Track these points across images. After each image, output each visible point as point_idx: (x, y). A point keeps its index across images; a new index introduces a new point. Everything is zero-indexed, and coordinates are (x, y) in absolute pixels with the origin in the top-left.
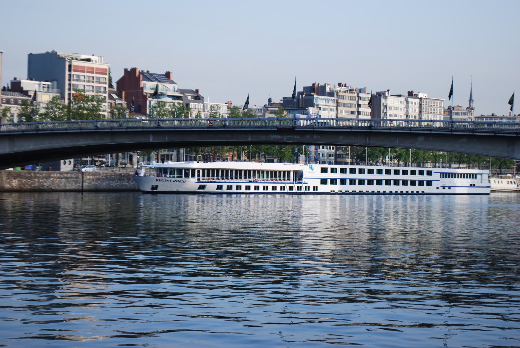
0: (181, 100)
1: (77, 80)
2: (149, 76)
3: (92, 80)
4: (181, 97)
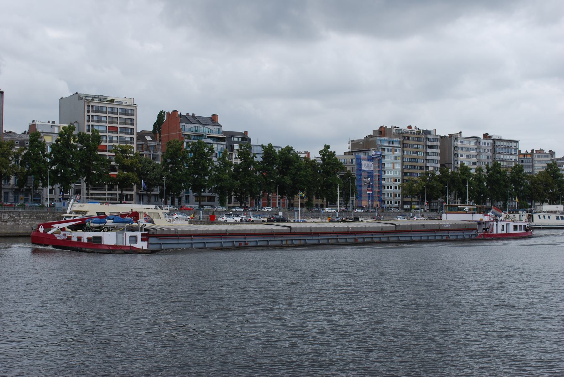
0: (224, 141)
1: (98, 121)
2: (186, 119)
3: (116, 121)
4: (225, 138)
